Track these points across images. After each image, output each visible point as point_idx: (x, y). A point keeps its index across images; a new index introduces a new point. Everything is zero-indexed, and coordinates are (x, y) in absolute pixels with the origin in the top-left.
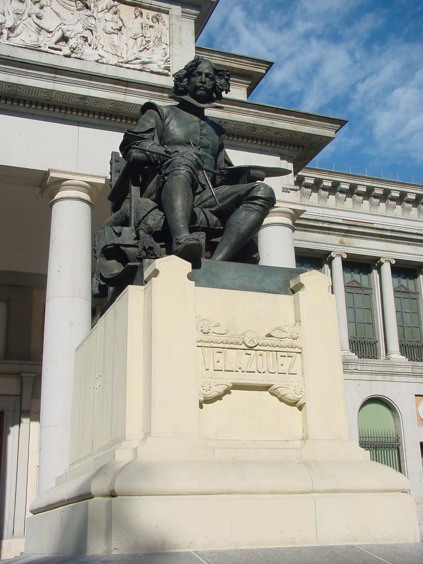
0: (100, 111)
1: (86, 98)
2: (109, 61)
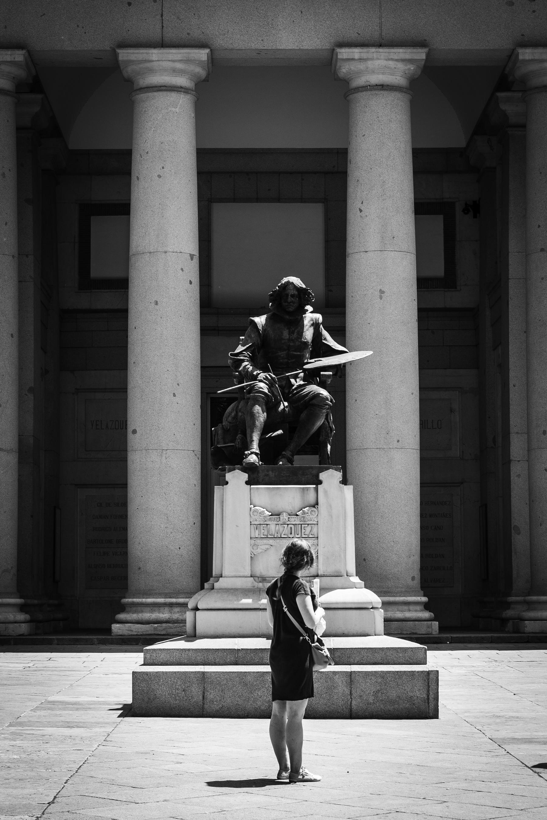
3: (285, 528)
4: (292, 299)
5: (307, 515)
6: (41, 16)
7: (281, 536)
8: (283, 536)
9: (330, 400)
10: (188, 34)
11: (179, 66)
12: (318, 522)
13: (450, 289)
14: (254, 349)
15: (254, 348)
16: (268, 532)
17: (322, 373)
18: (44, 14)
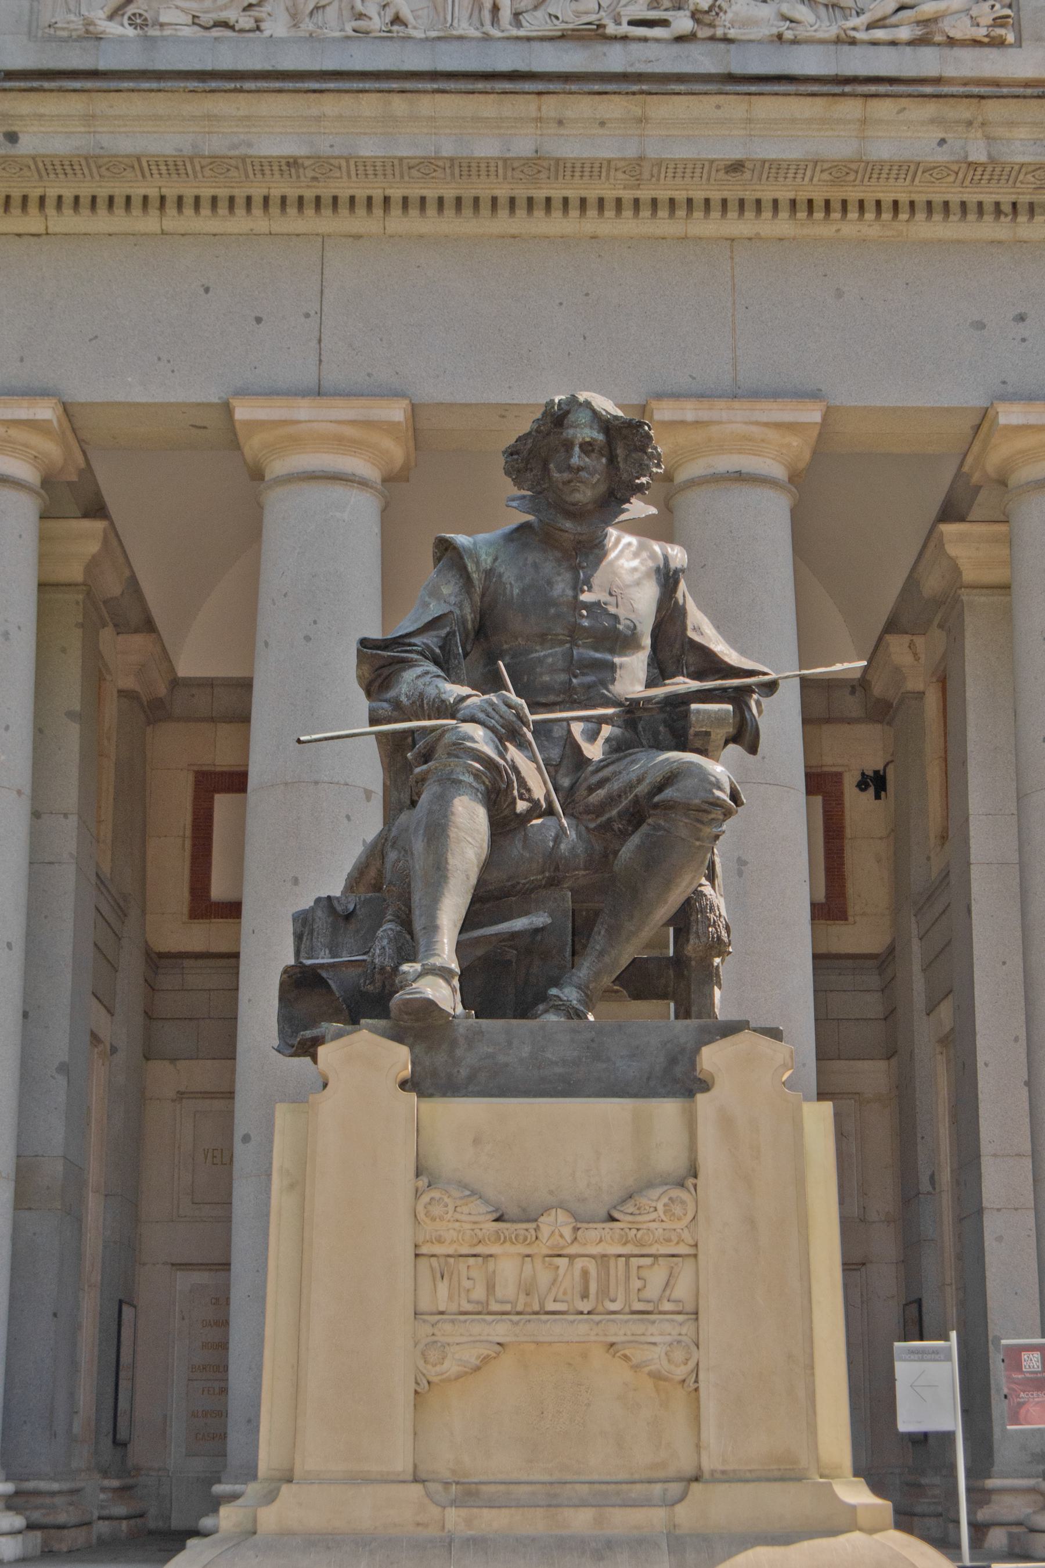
0: (792, 197)
1: (743, 166)
2: (815, 31)
3: (561, 1271)
4: (587, 460)
5: (654, 1216)
6: (90, 340)
7: (542, 1304)
8: (551, 1306)
9: (728, 792)
10: (369, 375)
11: (349, 431)
12: (696, 1245)
13: (837, 922)
14: (451, 634)
15: (448, 629)
16: (491, 1287)
17: (694, 706)
18: (96, 337)
